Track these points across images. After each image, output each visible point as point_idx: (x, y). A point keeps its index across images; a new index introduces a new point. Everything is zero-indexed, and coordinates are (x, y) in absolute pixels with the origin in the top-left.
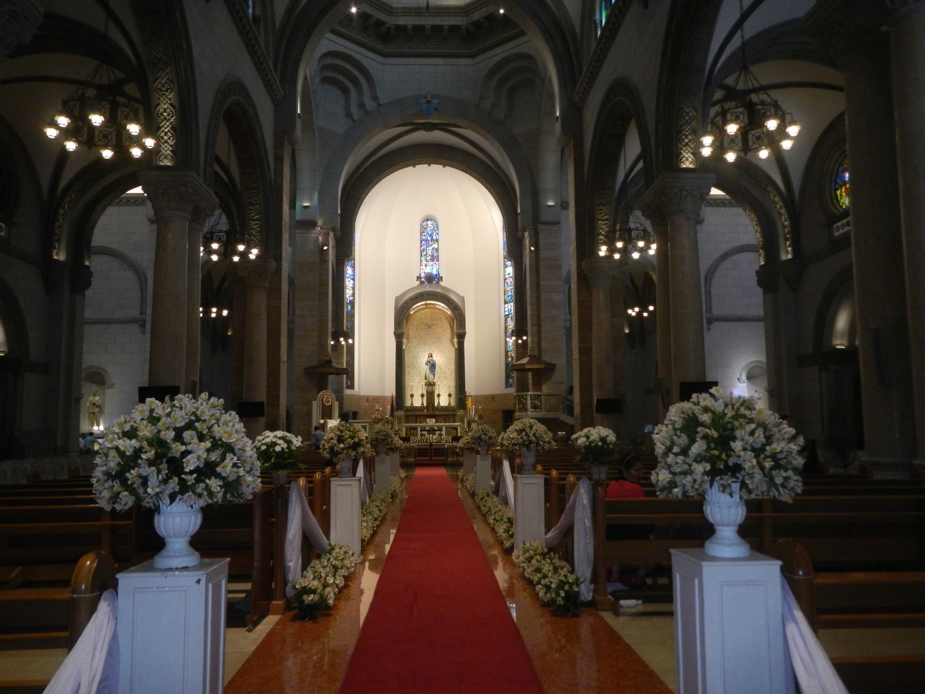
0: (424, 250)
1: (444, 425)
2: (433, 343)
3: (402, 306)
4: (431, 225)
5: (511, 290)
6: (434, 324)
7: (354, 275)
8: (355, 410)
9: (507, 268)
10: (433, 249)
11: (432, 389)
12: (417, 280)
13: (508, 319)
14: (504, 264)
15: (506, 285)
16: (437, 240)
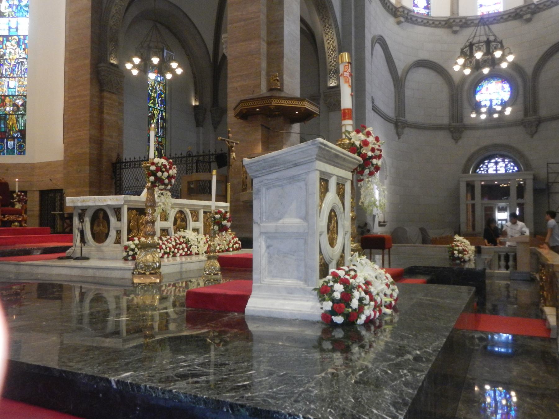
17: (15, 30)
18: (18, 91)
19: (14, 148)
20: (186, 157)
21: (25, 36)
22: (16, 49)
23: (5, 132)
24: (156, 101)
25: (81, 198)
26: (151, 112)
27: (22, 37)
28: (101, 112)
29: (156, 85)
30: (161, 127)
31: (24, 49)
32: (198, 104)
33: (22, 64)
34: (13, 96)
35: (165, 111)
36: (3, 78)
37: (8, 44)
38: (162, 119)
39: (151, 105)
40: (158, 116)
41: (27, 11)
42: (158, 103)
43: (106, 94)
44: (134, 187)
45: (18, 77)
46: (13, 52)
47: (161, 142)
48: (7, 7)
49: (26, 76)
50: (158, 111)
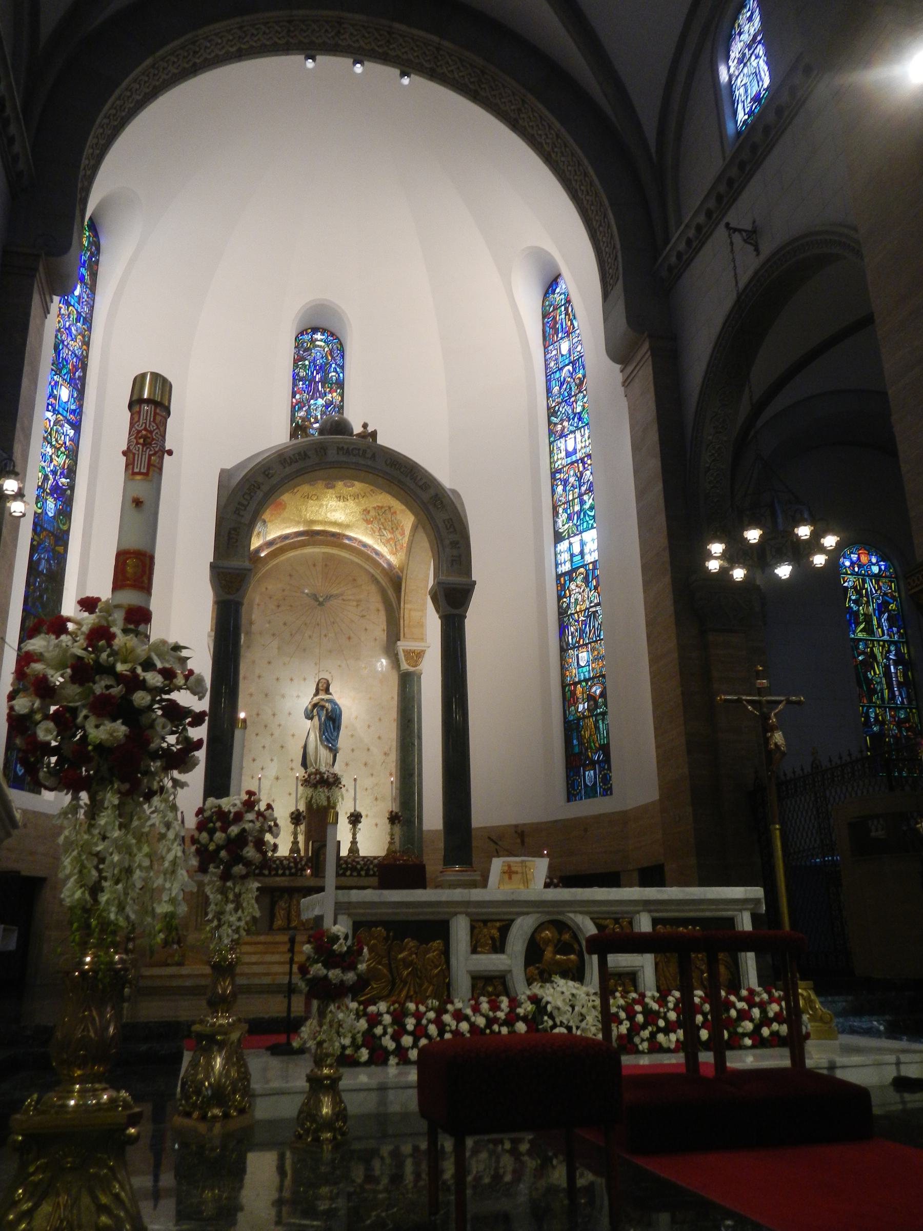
0: (300, 405)
1: (647, 905)
2: (330, 651)
3: (246, 479)
4: (322, 344)
5: (580, 495)
6: (331, 596)
7: (78, 412)
8: (41, 874)
9: (561, 444)
10: (327, 406)
11: (328, 798)
12: (293, 435)
13: (573, 586)
14: (551, 432)
15: (560, 489)
16: (340, 384)
17: (579, 557)
18: (593, 669)
19: (595, 782)
21: (594, 563)
22: (583, 591)
23: (580, 753)
24: (875, 622)
26: (863, 653)
27: (591, 566)
30: (899, 684)
31: (596, 588)
33: (595, 617)
34: (586, 680)
40: (888, 659)
41: (594, 517)
42: (880, 625)
45: (590, 643)
47: (907, 720)
48: (565, 521)
49: (602, 637)
50: (883, 647)
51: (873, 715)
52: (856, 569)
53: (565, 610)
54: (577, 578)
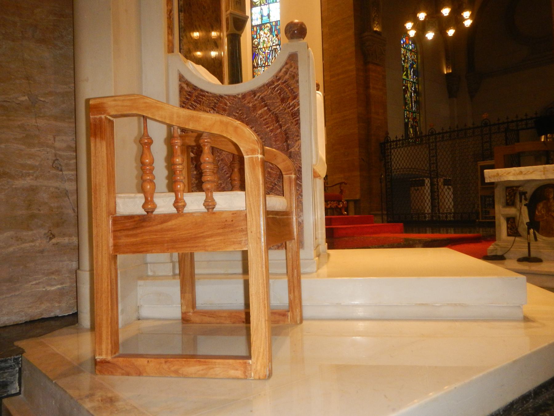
13: (262, 33)
17: (267, 17)
20: (429, 135)
21: (276, 22)
22: (269, 36)
25: (515, 170)
26: (404, 86)
28: (367, 87)
29: (408, 54)
30: (415, 102)
32: (451, 71)
33: (275, 51)
35: (418, 83)
36: (259, 68)
37: (262, 33)
38: (415, 92)
39: (404, 77)
40: (412, 90)
42: (410, 74)
43: (371, 66)
44: (405, 168)
46: (266, 39)
50: (411, 84)
51: (406, 114)
52: (405, 45)
53: (256, 45)
54: (265, 29)
